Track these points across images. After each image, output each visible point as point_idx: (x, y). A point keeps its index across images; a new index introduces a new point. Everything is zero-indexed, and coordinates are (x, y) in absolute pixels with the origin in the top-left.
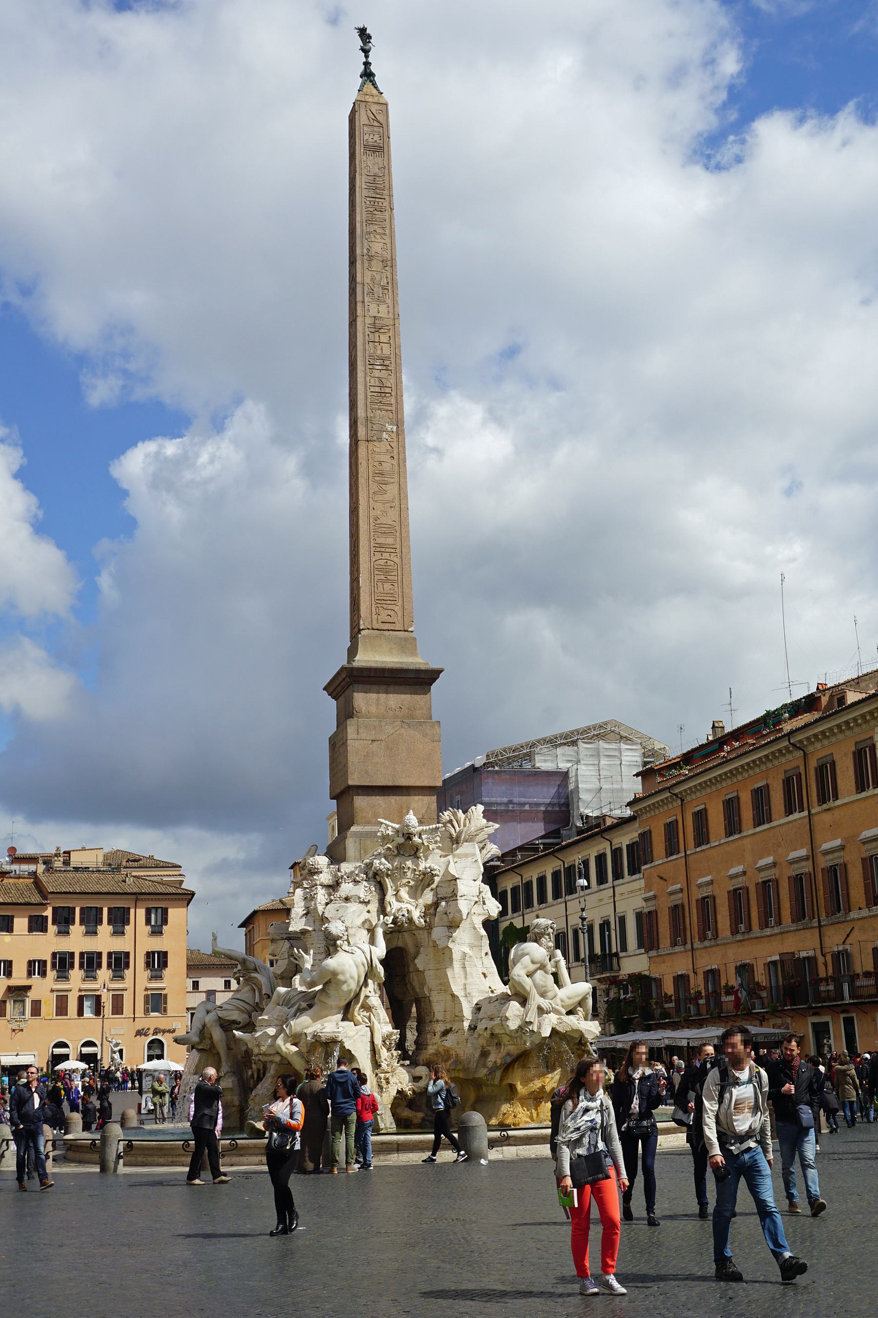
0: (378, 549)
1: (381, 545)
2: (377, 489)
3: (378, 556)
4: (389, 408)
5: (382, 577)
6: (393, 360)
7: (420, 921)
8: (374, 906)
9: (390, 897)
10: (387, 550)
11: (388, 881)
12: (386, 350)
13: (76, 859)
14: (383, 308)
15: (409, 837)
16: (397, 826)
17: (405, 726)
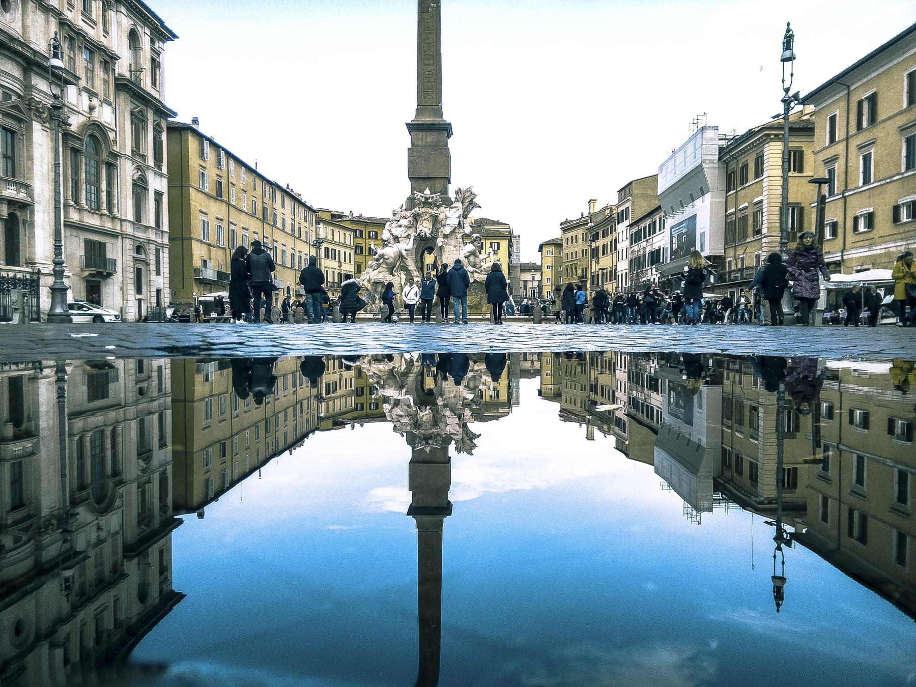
7: (428, 235)
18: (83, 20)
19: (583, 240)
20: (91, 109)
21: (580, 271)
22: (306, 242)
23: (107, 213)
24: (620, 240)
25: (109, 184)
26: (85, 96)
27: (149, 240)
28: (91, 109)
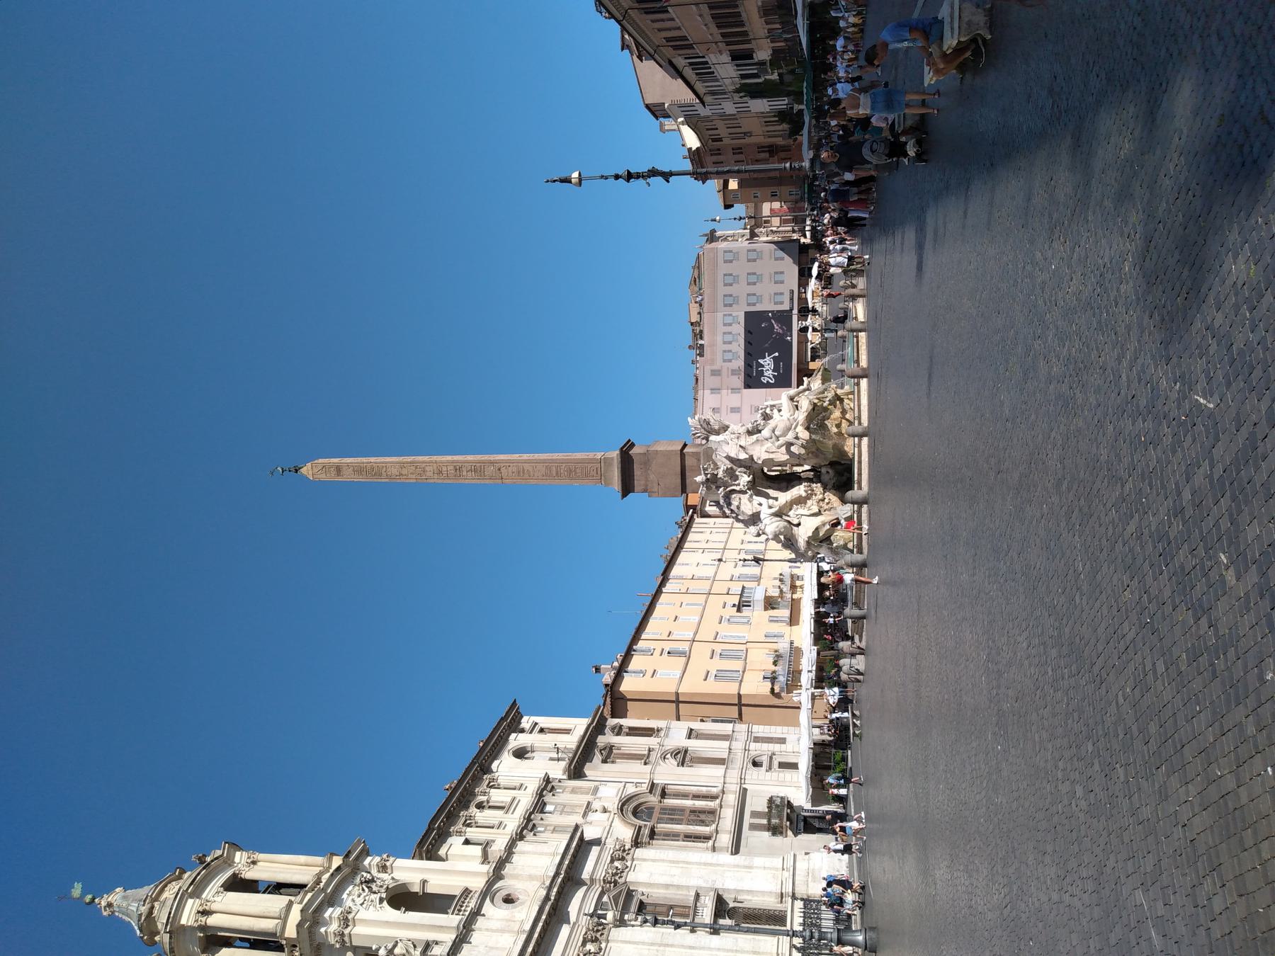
1: (557, 473)
6: (455, 464)
8: (742, 496)
9: (737, 488)
11: (728, 489)
12: (452, 468)
13: (695, 318)
14: (427, 469)
15: (707, 480)
18: (512, 813)
19: (720, 154)
20: (605, 811)
22: (730, 533)
23: (718, 801)
24: (723, 111)
25: (685, 796)
26: (591, 816)
27: (745, 750)
28: (605, 811)
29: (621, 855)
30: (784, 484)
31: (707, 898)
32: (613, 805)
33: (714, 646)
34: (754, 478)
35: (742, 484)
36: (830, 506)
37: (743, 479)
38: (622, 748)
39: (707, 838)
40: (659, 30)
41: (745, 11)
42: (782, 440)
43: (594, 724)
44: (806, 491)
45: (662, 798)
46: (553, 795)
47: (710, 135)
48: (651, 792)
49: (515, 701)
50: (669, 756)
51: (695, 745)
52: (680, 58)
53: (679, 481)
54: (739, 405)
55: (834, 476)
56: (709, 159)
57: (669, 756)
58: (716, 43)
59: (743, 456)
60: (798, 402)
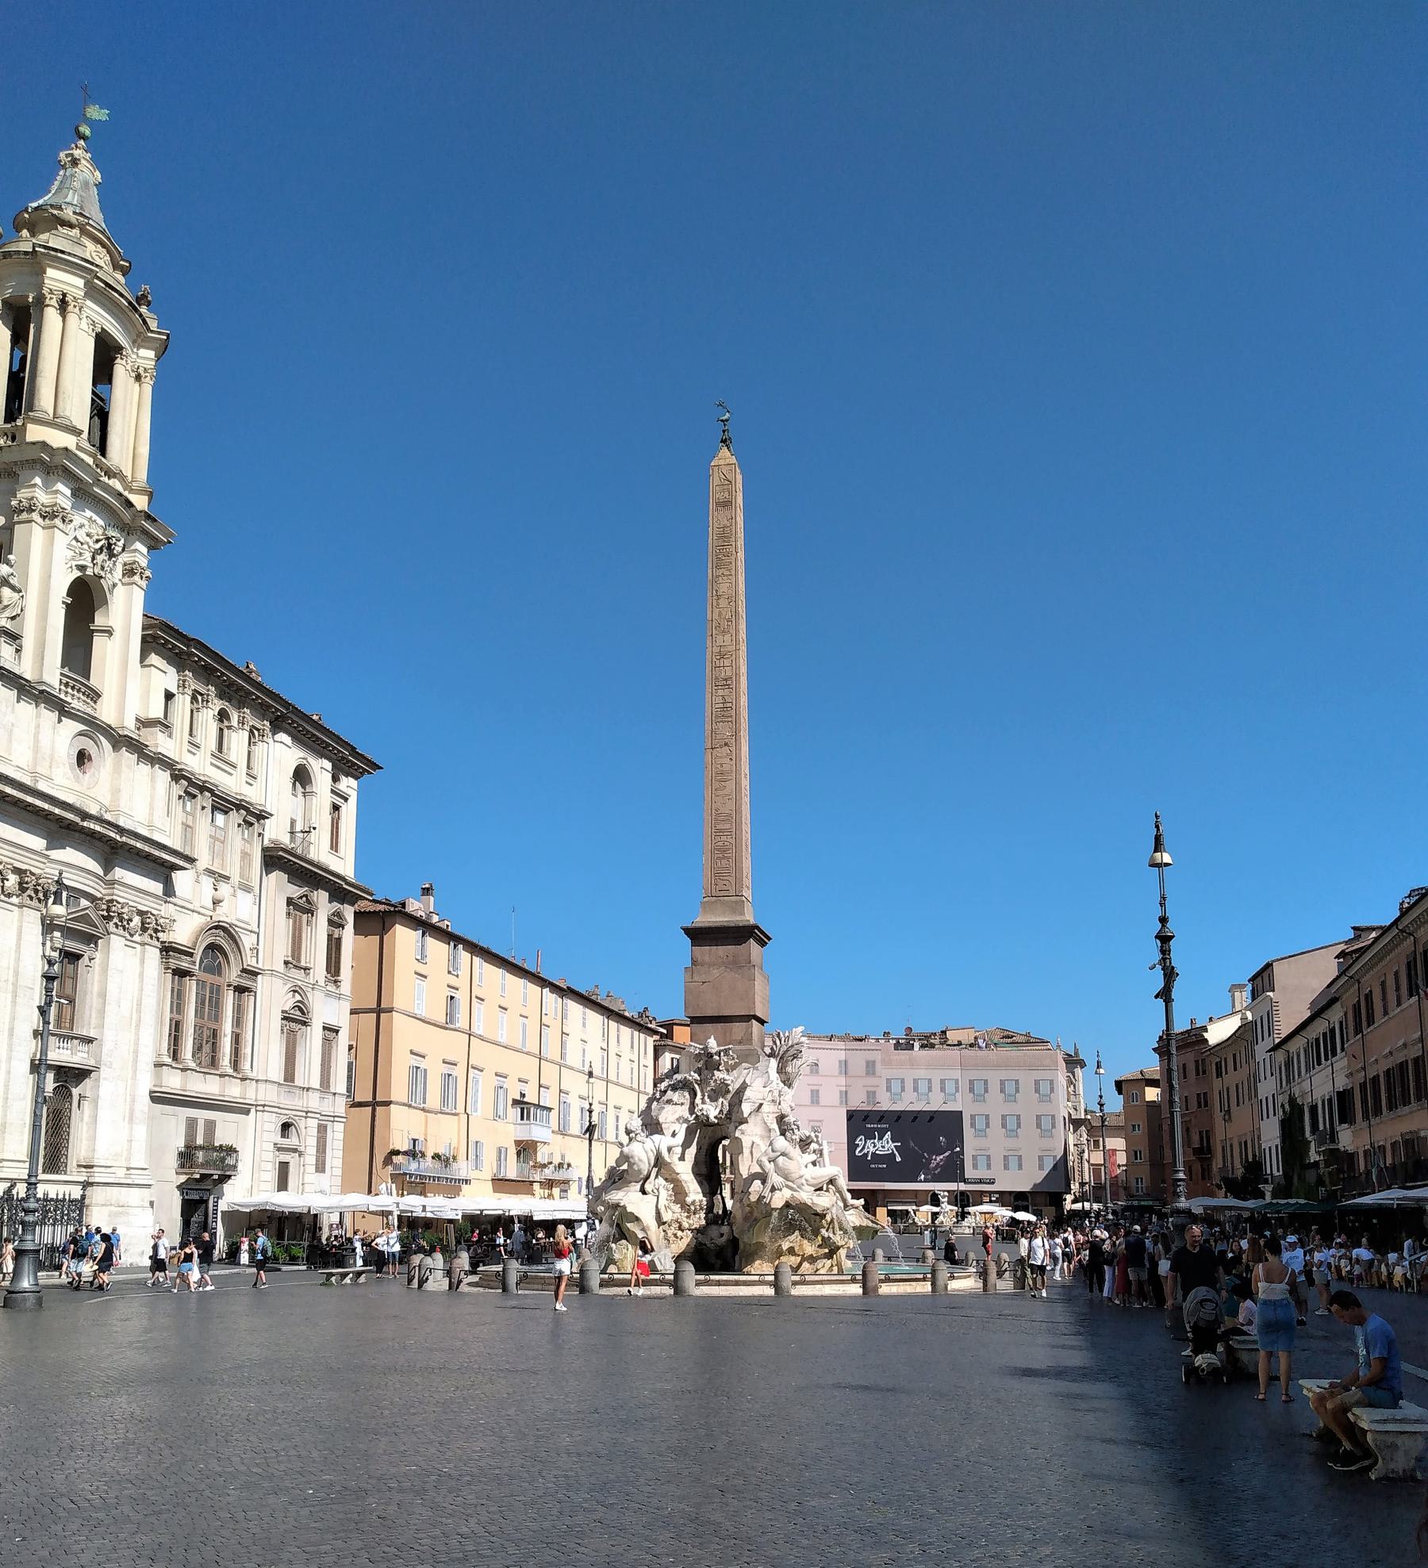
0: (718, 834)
1: (720, 831)
2: (718, 786)
3: (718, 838)
4: (730, 719)
5: (721, 856)
8: (687, 1107)
9: (698, 1100)
10: (725, 834)
13: (952, 1037)
16: (701, 1047)
17: (728, 970)
20: (216, 902)
21: (1196, 1138)
22: (632, 1089)
23: (230, 1071)
24: (1262, 1078)
25: (238, 1021)
26: (207, 882)
28: (216, 902)
29: (150, 926)
30: (704, 1170)
31: (86, 1055)
32: (224, 914)
33: (462, 1066)
34: (713, 1125)
35: (704, 1106)
36: (672, 1238)
37: (712, 1109)
38: (309, 928)
39: (175, 1056)
40: (1383, 984)
41: (1411, 1113)
42: (770, 1167)
43: (344, 886)
44: (693, 1203)
45: (235, 987)
46: (239, 825)
47: (1225, 1059)
48: (244, 971)
49: (382, 768)
50: (298, 997)
51: (314, 1036)
52: (1342, 1014)
53: (709, 1013)
54: (822, 1101)
55: (717, 1245)
56: (1190, 1058)
57: (298, 997)
58: (1364, 1069)
59: (746, 1108)
60: (827, 1191)
